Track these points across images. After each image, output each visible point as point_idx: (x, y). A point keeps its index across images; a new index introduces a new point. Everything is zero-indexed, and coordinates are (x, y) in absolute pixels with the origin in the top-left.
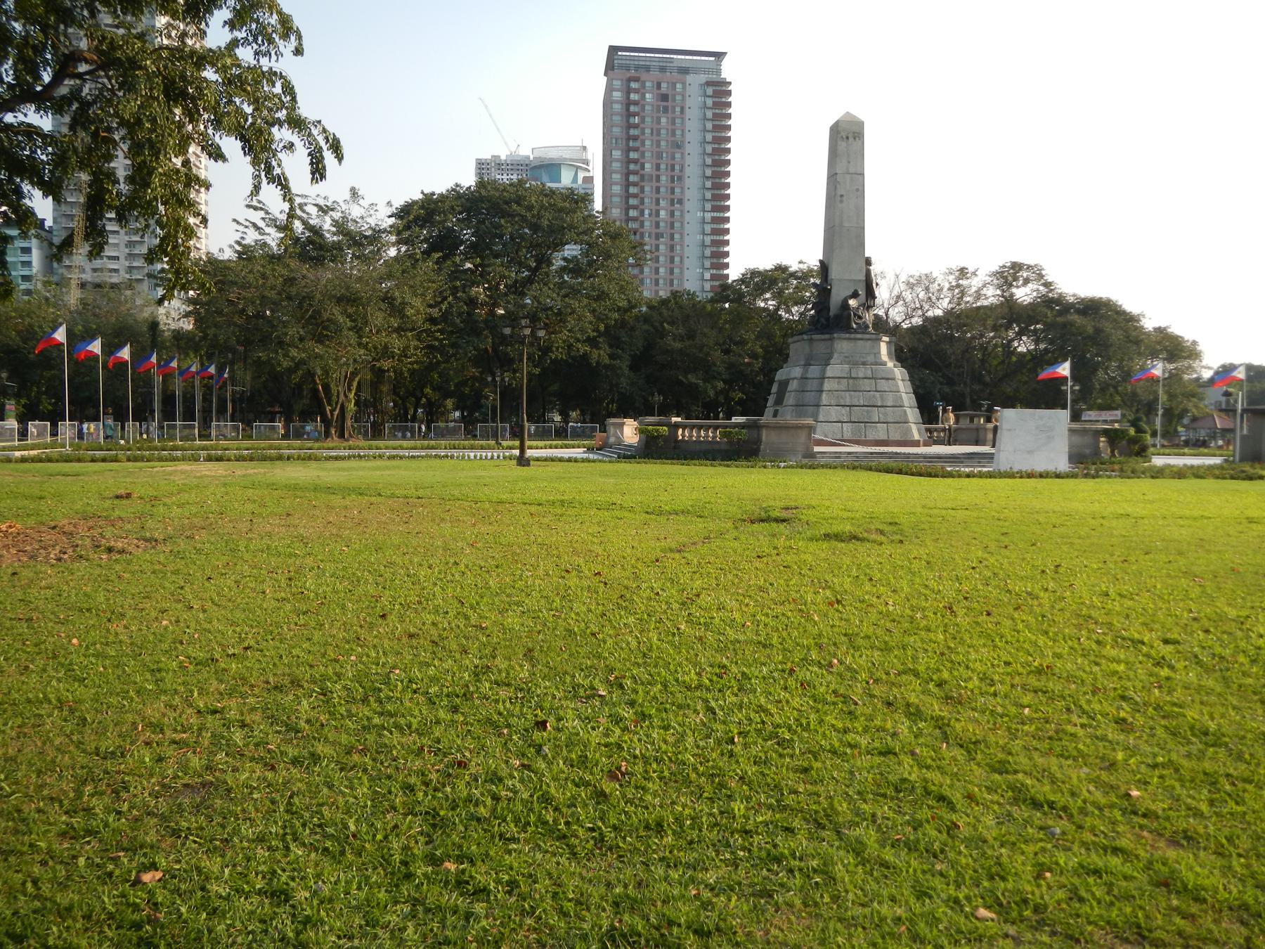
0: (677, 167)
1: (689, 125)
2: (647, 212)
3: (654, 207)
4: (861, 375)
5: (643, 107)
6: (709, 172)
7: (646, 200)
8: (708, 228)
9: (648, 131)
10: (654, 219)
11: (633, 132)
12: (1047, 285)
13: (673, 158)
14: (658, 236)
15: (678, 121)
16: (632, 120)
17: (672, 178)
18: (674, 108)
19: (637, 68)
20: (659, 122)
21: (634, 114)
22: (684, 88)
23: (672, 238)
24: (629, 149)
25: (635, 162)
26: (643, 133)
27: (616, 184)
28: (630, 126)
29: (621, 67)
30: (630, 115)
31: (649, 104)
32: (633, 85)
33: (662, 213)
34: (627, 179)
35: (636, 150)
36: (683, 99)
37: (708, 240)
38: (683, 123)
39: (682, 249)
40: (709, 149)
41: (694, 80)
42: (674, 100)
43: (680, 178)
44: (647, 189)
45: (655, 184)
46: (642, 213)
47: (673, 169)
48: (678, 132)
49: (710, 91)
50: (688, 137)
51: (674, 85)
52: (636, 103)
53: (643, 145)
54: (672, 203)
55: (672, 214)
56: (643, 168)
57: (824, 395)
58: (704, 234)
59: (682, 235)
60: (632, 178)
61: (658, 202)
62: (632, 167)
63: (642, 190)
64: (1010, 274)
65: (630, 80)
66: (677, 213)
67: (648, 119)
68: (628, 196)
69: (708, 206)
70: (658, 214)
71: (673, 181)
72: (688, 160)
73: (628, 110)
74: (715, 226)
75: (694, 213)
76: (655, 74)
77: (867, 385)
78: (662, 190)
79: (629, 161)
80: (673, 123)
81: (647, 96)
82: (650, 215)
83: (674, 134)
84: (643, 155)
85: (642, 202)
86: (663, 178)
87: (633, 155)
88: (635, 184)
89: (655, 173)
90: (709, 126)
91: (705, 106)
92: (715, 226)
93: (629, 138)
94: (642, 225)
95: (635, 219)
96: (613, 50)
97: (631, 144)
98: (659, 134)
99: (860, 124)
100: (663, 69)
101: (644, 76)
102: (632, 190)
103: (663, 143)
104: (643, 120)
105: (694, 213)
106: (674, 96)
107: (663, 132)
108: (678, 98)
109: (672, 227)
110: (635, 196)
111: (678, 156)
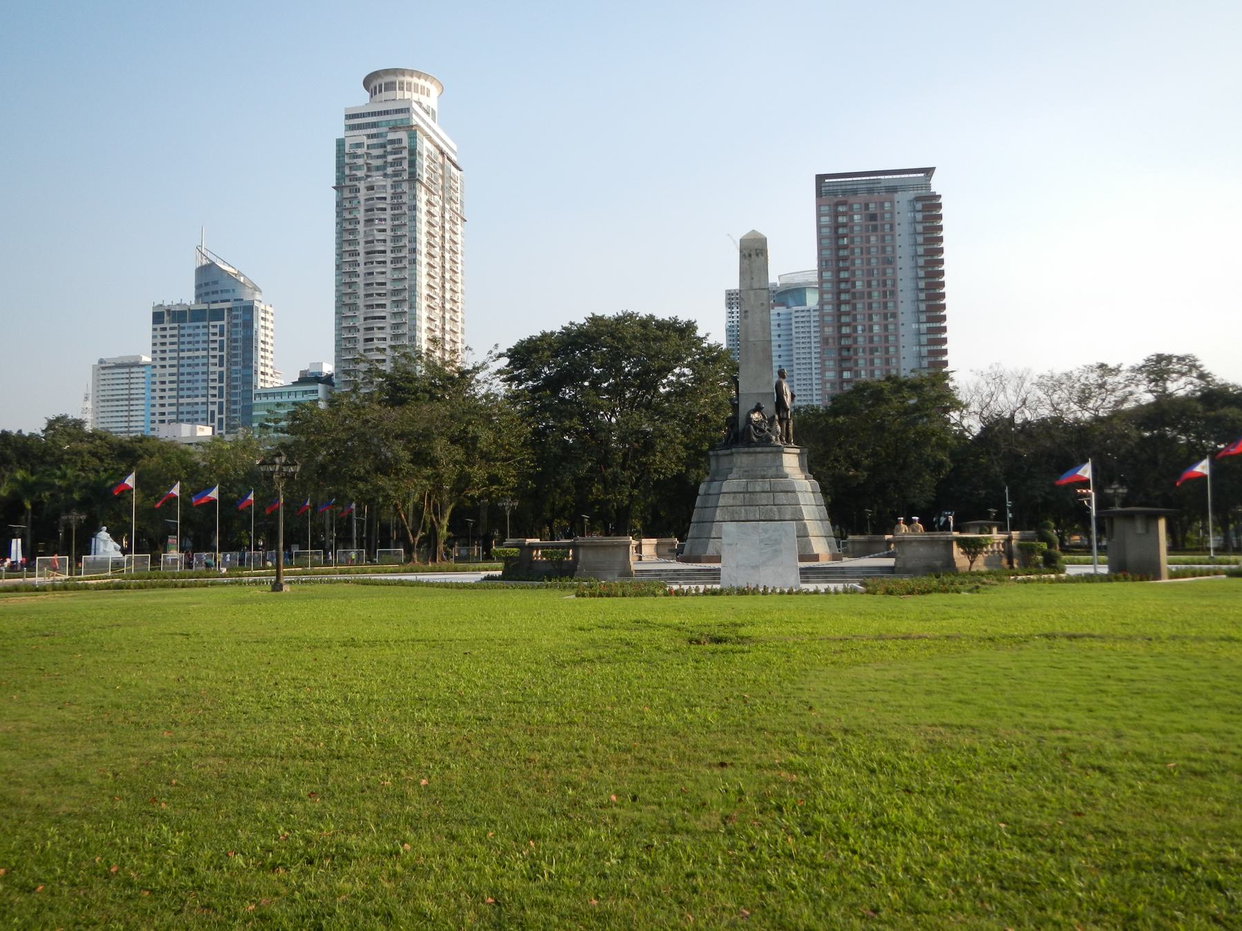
0: (889, 282)
1: (899, 241)
2: (860, 328)
3: (867, 323)
4: (758, 489)
5: (852, 231)
6: (922, 284)
7: (859, 317)
8: (924, 339)
9: (857, 251)
10: (867, 334)
11: (842, 253)
12: (1202, 376)
13: (884, 274)
14: (872, 351)
15: (888, 238)
16: (841, 242)
17: (885, 293)
18: (883, 226)
19: (845, 192)
20: (868, 241)
21: (843, 236)
22: (892, 206)
23: (887, 351)
24: (839, 270)
25: (846, 281)
26: (853, 252)
27: (828, 303)
28: (839, 248)
29: (828, 193)
30: (839, 237)
31: (857, 225)
32: (841, 209)
33: (876, 328)
34: (838, 298)
35: (846, 269)
36: (892, 217)
37: (925, 350)
38: (893, 239)
39: (898, 361)
40: (921, 262)
41: (903, 198)
42: (883, 218)
43: (893, 293)
44: (859, 306)
45: (867, 301)
46: (855, 329)
47: (885, 284)
48: (889, 249)
49: (919, 206)
50: (899, 252)
51: (882, 204)
52: (844, 225)
53: (853, 264)
54: (886, 317)
55: (886, 328)
56: (854, 285)
57: (718, 511)
58: (920, 345)
59: (897, 347)
60: (843, 297)
61: (870, 318)
62: (843, 286)
64: (1159, 368)
66: (891, 327)
67: (857, 240)
68: (840, 314)
69: (923, 317)
70: (871, 329)
71: (885, 295)
72: (900, 274)
73: (836, 232)
74: (932, 336)
75: (908, 325)
76: (863, 197)
77: (763, 499)
79: (840, 281)
80: (883, 240)
81: (856, 217)
83: (884, 250)
84: (853, 274)
85: (855, 319)
86: (875, 294)
87: (843, 275)
88: (847, 302)
90: (920, 239)
91: (915, 221)
92: (932, 336)
93: (839, 259)
94: (855, 341)
95: (848, 336)
96: (820, 179)
97: (841, 264)
98: (869, 252)
99: (763, 241)
100: (870, 191)
101: (851, 199)
102: (844, 308)
103: (873, 261)
104: (852, 241)
105: (908, 325)
106: (883, 215)
107: (873, 250)
108: (887, 216)
109: (887, 340)
110: (847, 314)
111: (889, 271)
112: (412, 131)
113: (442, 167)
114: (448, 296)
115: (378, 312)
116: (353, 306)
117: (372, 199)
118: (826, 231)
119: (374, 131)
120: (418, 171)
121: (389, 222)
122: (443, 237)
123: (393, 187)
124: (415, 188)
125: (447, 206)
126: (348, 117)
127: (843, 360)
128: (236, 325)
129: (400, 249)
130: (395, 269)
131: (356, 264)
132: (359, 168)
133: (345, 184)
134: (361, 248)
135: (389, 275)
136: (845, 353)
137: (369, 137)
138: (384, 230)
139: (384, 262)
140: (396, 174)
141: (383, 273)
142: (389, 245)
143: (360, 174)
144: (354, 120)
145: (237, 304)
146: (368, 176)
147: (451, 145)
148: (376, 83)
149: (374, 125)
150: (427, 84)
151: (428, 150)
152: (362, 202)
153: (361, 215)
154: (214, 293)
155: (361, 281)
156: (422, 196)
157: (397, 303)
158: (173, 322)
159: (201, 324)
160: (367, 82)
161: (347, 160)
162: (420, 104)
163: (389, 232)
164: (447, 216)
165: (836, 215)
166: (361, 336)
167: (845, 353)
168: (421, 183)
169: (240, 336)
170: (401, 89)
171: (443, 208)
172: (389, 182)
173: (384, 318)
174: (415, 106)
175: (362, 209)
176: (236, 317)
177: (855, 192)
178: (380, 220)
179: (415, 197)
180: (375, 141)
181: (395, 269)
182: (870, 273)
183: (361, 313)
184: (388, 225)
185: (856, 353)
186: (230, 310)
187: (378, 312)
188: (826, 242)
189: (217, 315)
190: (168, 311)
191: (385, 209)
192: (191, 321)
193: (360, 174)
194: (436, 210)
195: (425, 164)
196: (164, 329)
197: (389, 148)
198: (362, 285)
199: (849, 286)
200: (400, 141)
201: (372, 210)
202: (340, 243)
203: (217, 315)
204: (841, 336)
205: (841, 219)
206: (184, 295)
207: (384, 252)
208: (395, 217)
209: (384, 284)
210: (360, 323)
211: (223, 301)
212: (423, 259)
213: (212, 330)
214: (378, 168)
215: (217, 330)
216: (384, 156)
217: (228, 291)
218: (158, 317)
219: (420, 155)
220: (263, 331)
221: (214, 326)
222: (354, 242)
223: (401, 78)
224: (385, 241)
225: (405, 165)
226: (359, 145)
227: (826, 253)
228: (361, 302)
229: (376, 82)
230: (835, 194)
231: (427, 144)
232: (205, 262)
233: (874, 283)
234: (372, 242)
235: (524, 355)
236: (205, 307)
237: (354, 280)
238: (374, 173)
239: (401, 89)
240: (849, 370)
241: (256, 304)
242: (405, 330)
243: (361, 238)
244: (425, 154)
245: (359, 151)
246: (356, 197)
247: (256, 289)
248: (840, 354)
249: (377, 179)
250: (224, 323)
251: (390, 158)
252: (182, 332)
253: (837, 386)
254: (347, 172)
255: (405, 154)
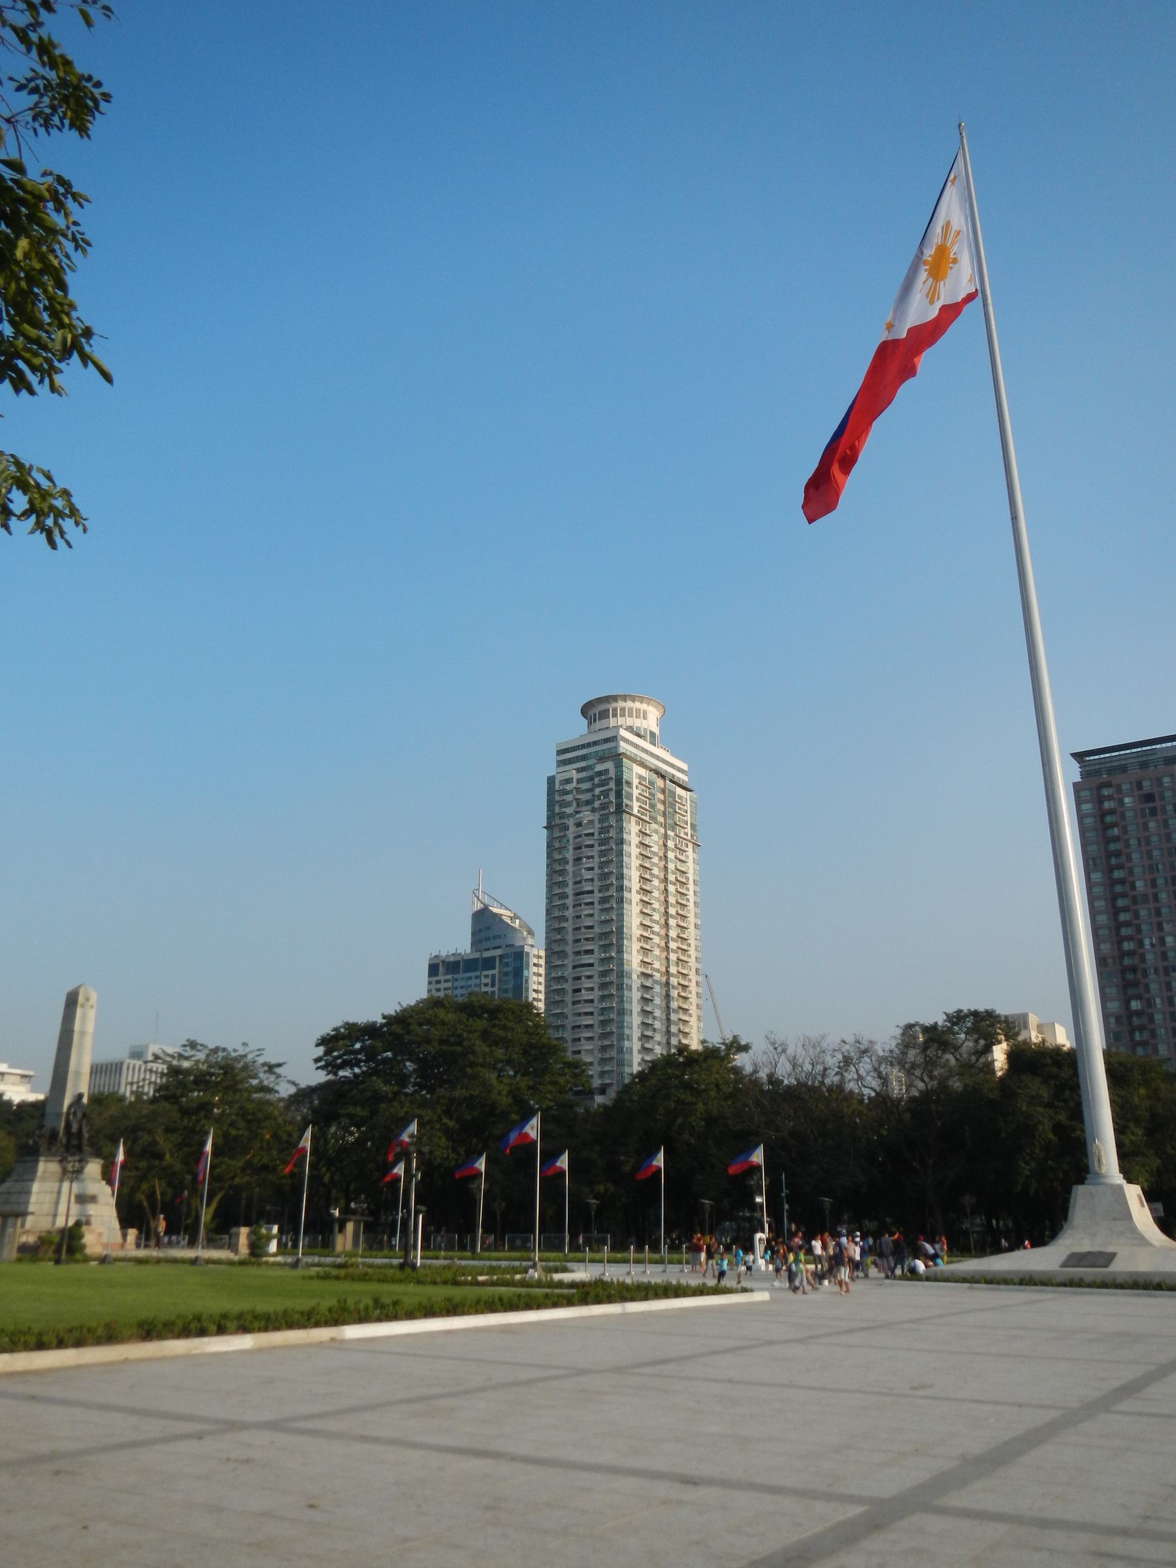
5: (1123, 817)
9: (1133, 842)
18: (1163, 808)
19: (1110, 771)
21: (1113, 825)
24: (1111, 869)
25: (1122, 882)
26: (1128, 845)
30: (1106, 827)
32: (1106, 792)
35: (1120, 867)
42: (1163, 798)
45: (1152, 905)
46: (1141, 944)
51: (1159, 781)
52: (1112, 812)
53: (1129, 859)
56: (1133, 887)
60: (1120, 903)
61: (1160, 927)
62: (1118, 888)
63: (1137, 916)
65: (1101, 786)
67: (1131, 828)
68: (1119, 926)
73: (1102, 822)
78: (1164, 911)
79: (1114, 882)
81: (1127, 800)
82: (1152, 945)
84: (1131, 872)
85: (1139, 930)
87: (1118, 874)
88: (1126, 909)
89: (1150, 891)
94: (1143, 959)
95: (1131, 953)
97: (1113, 861)
98: (1148, 842)
100: (1144, 765)
102: (1123, 917)
103: (1156, 853)
104: (1125, 830)
107: (1154, 839)
110: (1127, 924)
112: (617, 758)
113: (663, 791)
114: (673, 933)
115: (587, 959)
116: (562, 954)
117: (580, 836)
118: (1089, 821)
119: (583, 764)
120: (625, 801)
121: (597, 859)
122: (666, 868)
123: (601, 821)
124: (621, 820)
125: (669, 833)
126: (559, 753)
127: (1126, 985)
128: (506, 974)
129: (606, 888)
130: (602, 910)
131: (564, 907)
132: (568, 804)
133: (555, 823)
134: (569, 890)
135: (596, 917)
136: (1130, 976)
137: (579, 770)
138: (592, 869)
139: (592, 903)
140: (604, 807)
141: (592, 915)
142: (597, 883)
143: (569, 810)
144: (566, 755)
145: (509, 950)
146: (577, 812)
147: (677, 766)
148: (591, 713)
149: (584, 758)
150: (644, 706)
151: (641, 777)
152: (571, 841)
153: (570, 855)
154: (487, 939)
155: (569, 925)
156: (632, 830)
157: (606, 948)
158: (447, 973)
159: (473, 974)
160: (585, 710)
161: (557, 798)
162: (630, 729)
163: (596, 871)
164: (670, 844)
165: (1100, 800)
166: (568, 986)
167: (1130, 976)
168: (631, 814)
169: (510, 986)
170: (623, 715)
171: (666, 837)
172: (597, 816)
173: (591, 965)
174: (623, 733)
175: (571, 848)
176: (507, 965)
177: (1123, 769)
178: (588, 858)
179: (621, 830)
180: (584, 774)
181: (602, 910)
182: (1153, 868)
183: (569, 962)
184: (594, 864)
185: (1145, 974)
186: (501, 957)
187: (587, 959)
188: (1091, 835)
189: (489, 963)
190: (443, 962)
191: (592, 846)
192: (484, 969)
193: (569, 810)
194: (654, 842)
195: (636, 793)
196: (438, 982)
197: (596, 780)
198: (570, 930)
199: (1127, 887)
200: (607, 771)
201: (580, 848)
202: (551, 885)
203: (489, 963)
204: (1123, 954)
205: (1107, 805)
206: (459, 943)
207: (592, 892)
208: (603, 854)
209: (591, 927)
210: (568, 972)
211: (494, 948)
212: (633, 897)
213: (484, 981)
214: (588, 803)
215: (488, 981)
216: (591, 790)
217: (499, 937)
218: (433, 969)
219: (629, 784)
220: (535, 978)
221: (486, 976)
222: (563, 884)
223: (614, 705)
224: (592, 880)
225: (612, 798)
226: (568, 781)
227: (1093, 848)
228: (569, 949)
229: (595, 710)
230: (1097, 773)
231: (638, 770)
232: (480, 906)
233: (1160, 881)
234: (580, 882)
235: (339, 1044)
236: (477, 955)
237: (565, 925)
238: (584, 809)
239: (615, 715)
240: (1138, 997)
241: (527, 949)
242: (613, 977)
243: (570, 880)
244: (635, 782)
245: (568, 787)
246: (565, 836)
247: (531, 933)
248: (1123, 979)
249: (586, 815)
250: (495, 972)
251: (597, 791)
252: (456, 984)
253: (1125, 1021)
254: (557, 810)
255: (612, 785)
